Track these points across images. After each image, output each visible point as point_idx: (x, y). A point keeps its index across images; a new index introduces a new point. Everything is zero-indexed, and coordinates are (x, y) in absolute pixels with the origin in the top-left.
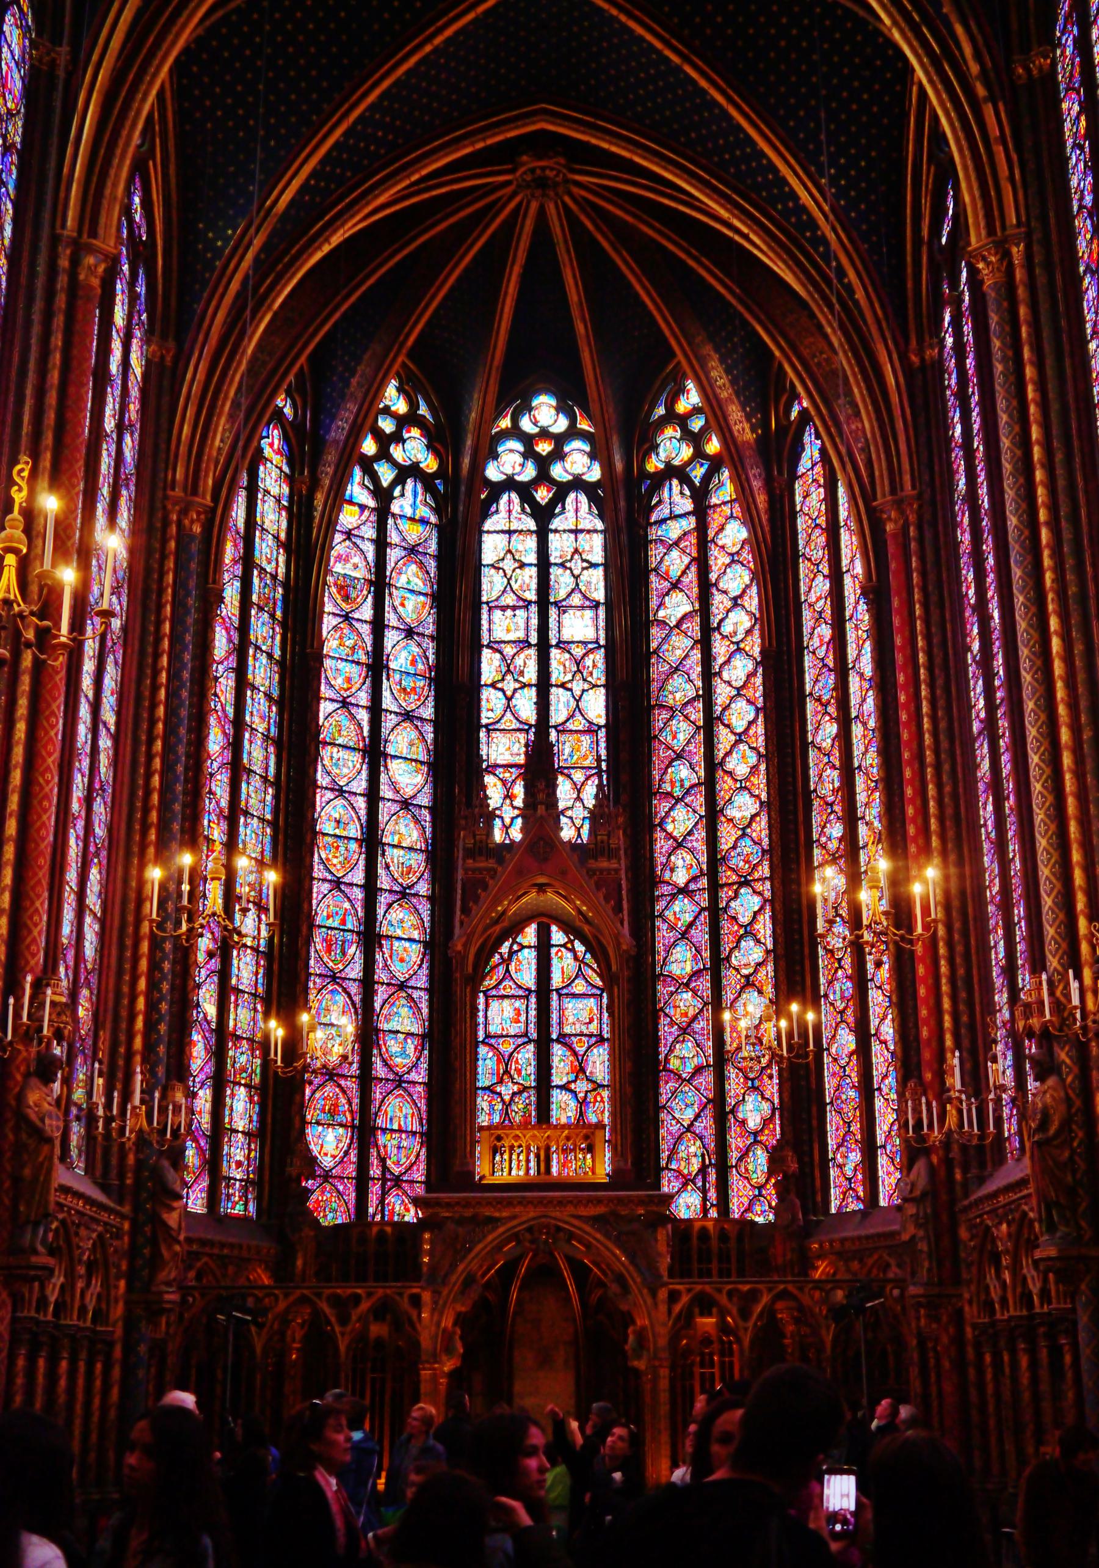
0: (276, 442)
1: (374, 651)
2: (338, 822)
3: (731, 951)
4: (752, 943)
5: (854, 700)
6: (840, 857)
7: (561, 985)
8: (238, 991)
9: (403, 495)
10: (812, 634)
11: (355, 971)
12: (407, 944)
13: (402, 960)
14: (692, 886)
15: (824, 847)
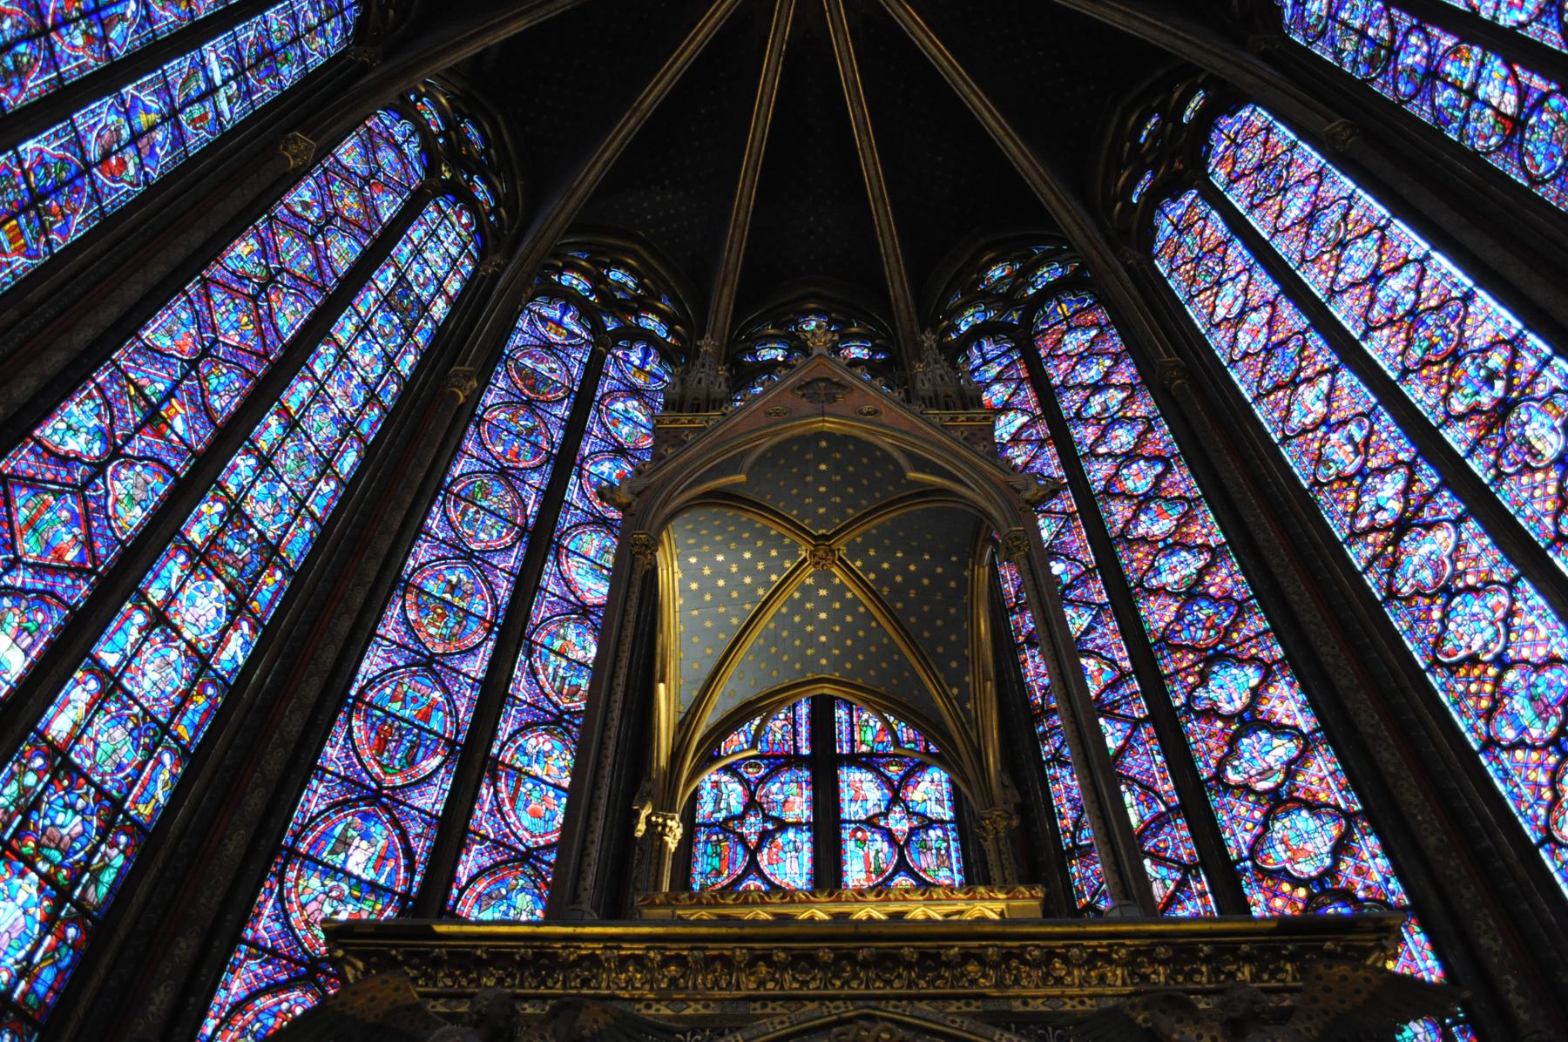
0: (464, 220)
1: (562, 446)
2: (453, 588)
3: (1222, 764)
4: (1264, 735)
5: (1348, 326)
6: (1420, 508)
7: (866, 885)
8: (111, 685)
9: (630, 348)
10: (1234, 341)
11: (431, 800)
12: (551, 794)
13: (535, 814)
14: (1111, 697)
15: (1372, 529)
